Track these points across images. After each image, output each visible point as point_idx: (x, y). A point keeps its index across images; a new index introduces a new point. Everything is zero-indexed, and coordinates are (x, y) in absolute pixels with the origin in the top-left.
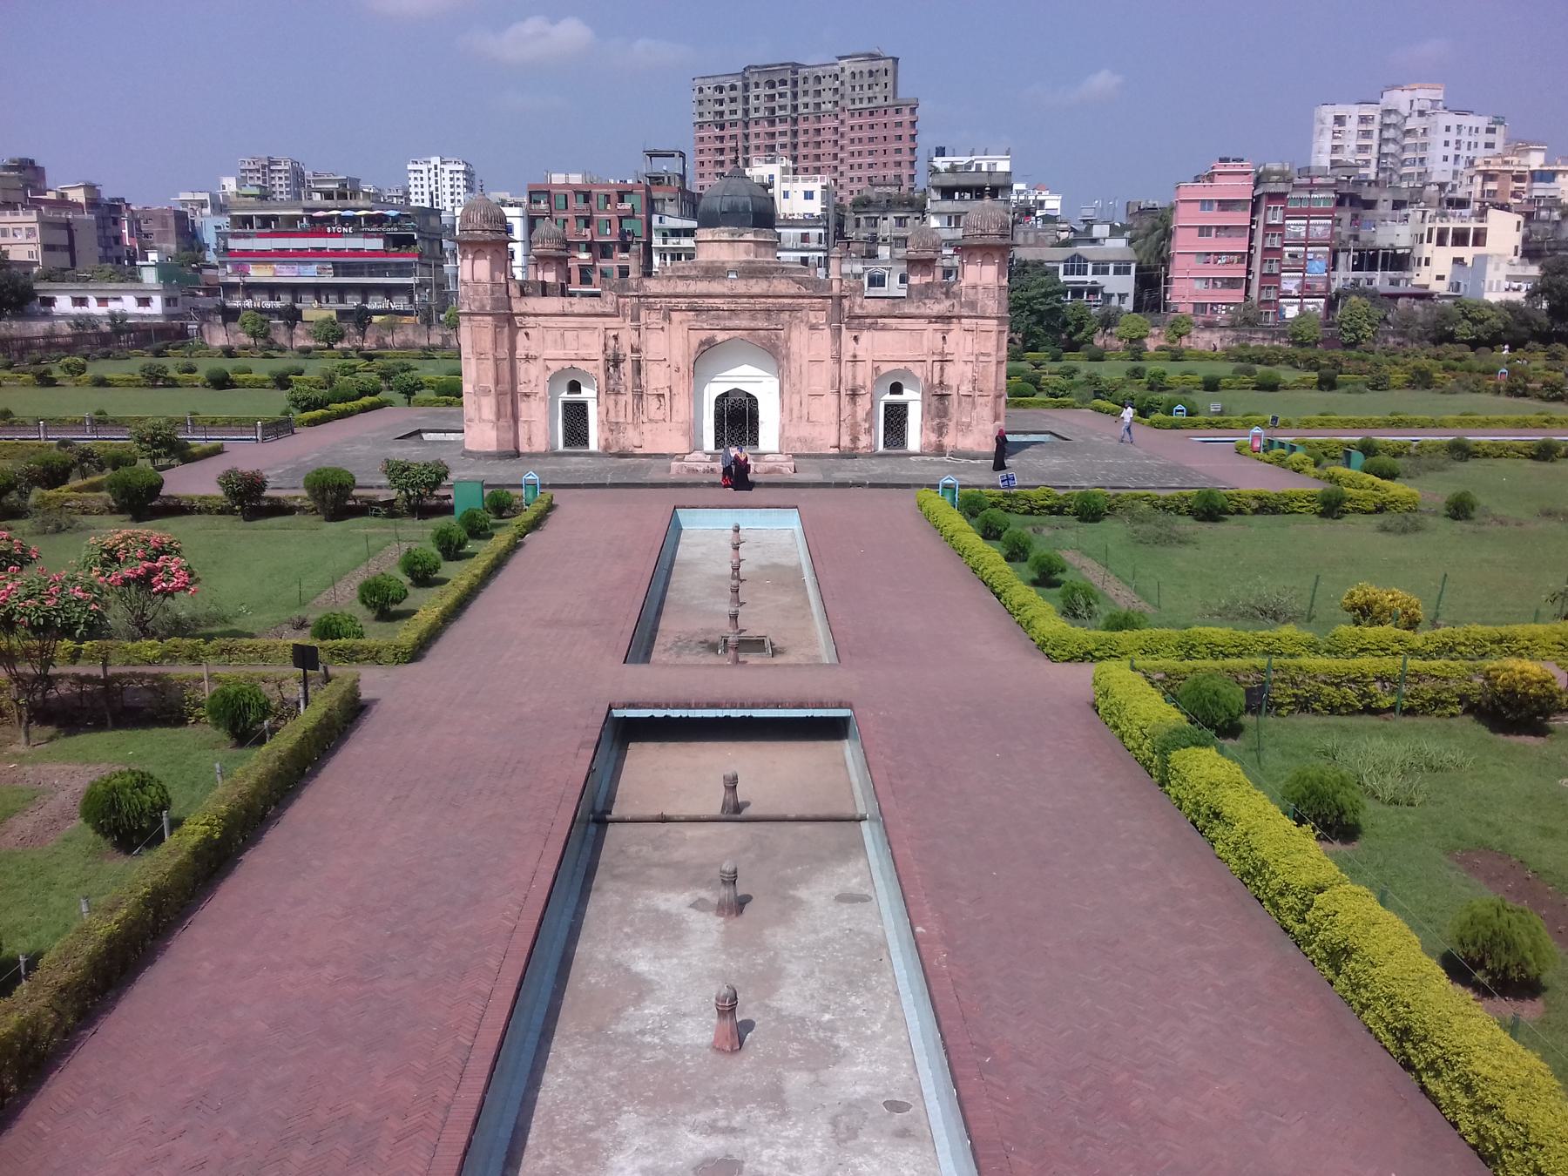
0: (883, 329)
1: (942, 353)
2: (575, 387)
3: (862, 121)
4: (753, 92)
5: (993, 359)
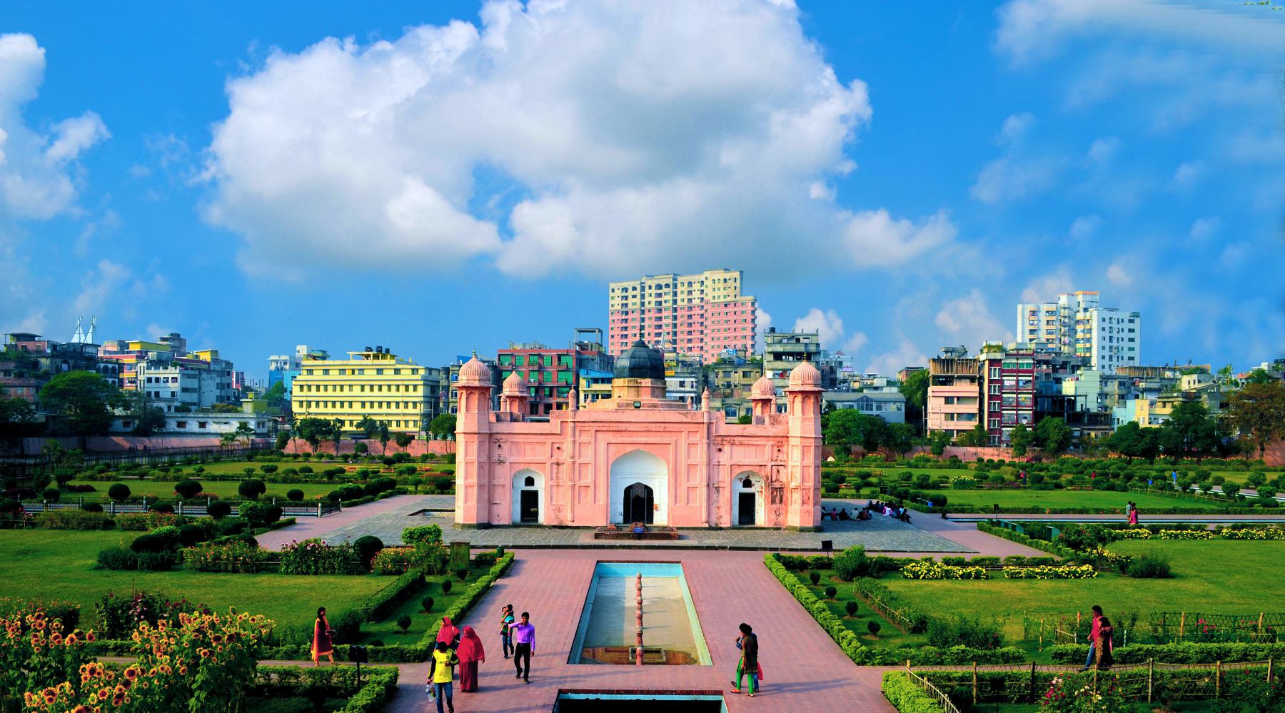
2: (530, 481)
4: (647, 291)
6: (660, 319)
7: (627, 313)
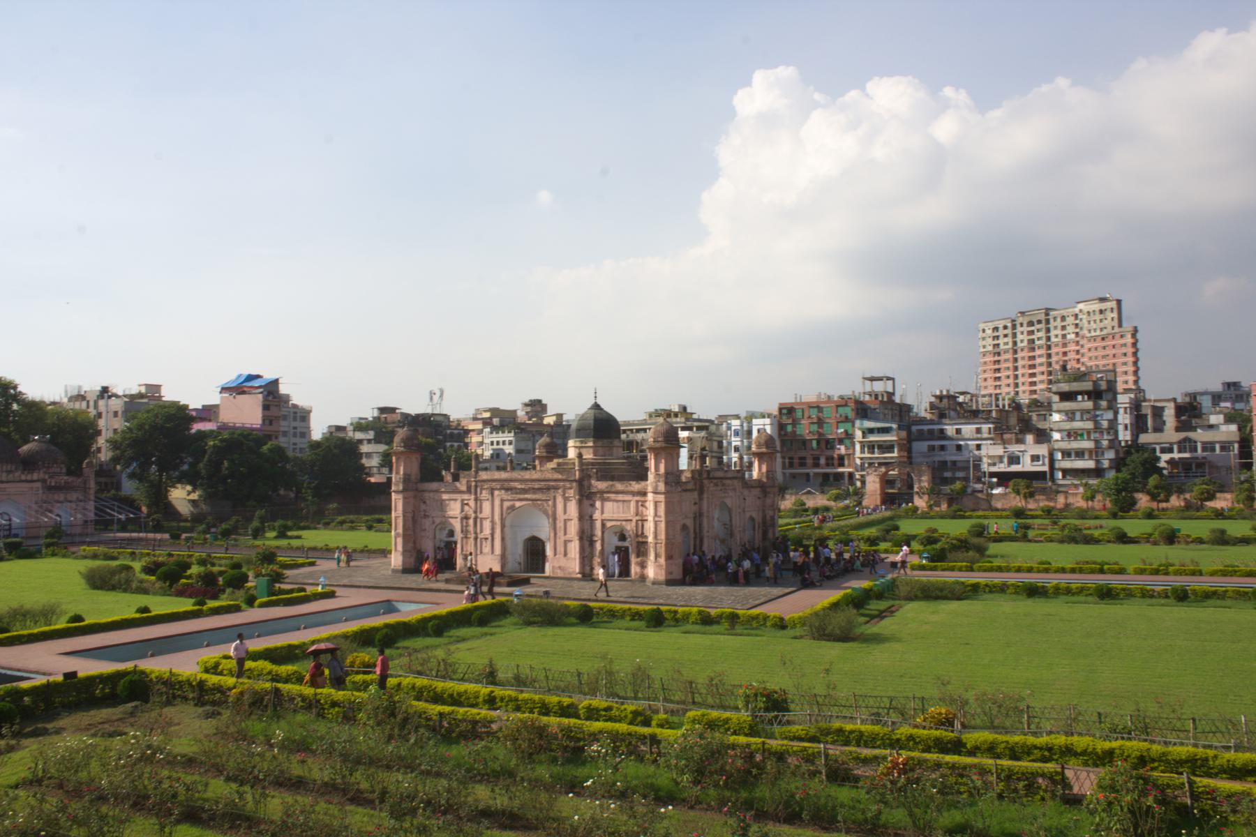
0: (608, 500)
1: (642, 515)
3: (1096, 345)
4: (1019, 329)
5: (663, 519)
6: (1033, 358)
7: (999, 354)
